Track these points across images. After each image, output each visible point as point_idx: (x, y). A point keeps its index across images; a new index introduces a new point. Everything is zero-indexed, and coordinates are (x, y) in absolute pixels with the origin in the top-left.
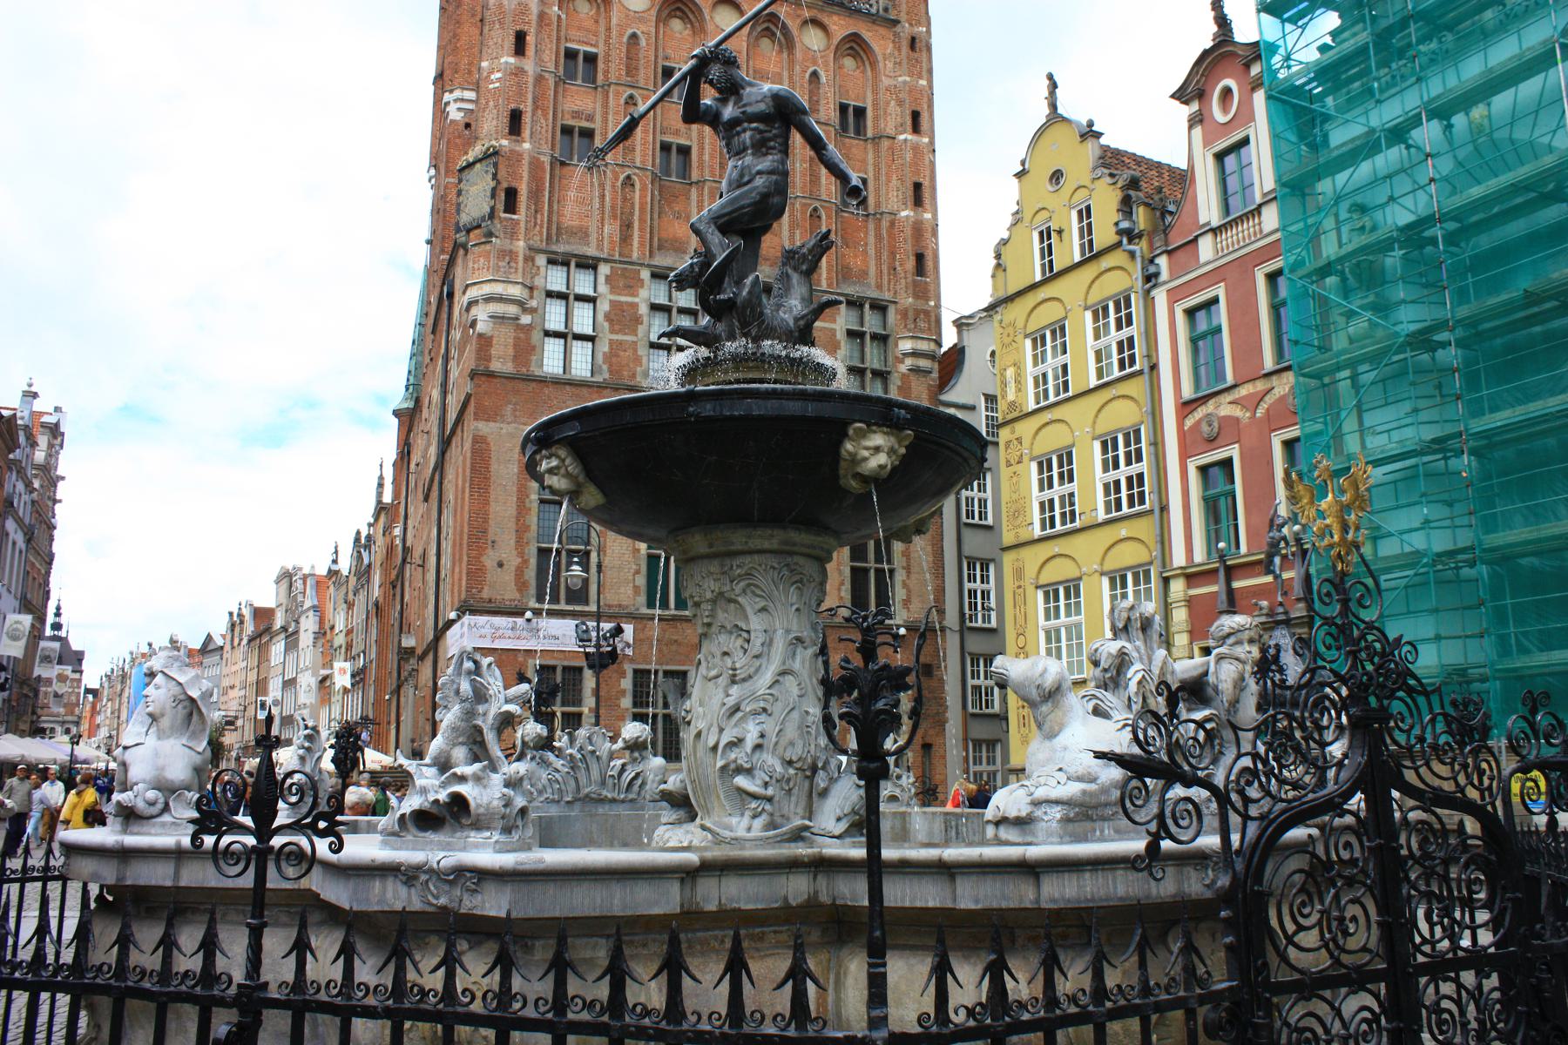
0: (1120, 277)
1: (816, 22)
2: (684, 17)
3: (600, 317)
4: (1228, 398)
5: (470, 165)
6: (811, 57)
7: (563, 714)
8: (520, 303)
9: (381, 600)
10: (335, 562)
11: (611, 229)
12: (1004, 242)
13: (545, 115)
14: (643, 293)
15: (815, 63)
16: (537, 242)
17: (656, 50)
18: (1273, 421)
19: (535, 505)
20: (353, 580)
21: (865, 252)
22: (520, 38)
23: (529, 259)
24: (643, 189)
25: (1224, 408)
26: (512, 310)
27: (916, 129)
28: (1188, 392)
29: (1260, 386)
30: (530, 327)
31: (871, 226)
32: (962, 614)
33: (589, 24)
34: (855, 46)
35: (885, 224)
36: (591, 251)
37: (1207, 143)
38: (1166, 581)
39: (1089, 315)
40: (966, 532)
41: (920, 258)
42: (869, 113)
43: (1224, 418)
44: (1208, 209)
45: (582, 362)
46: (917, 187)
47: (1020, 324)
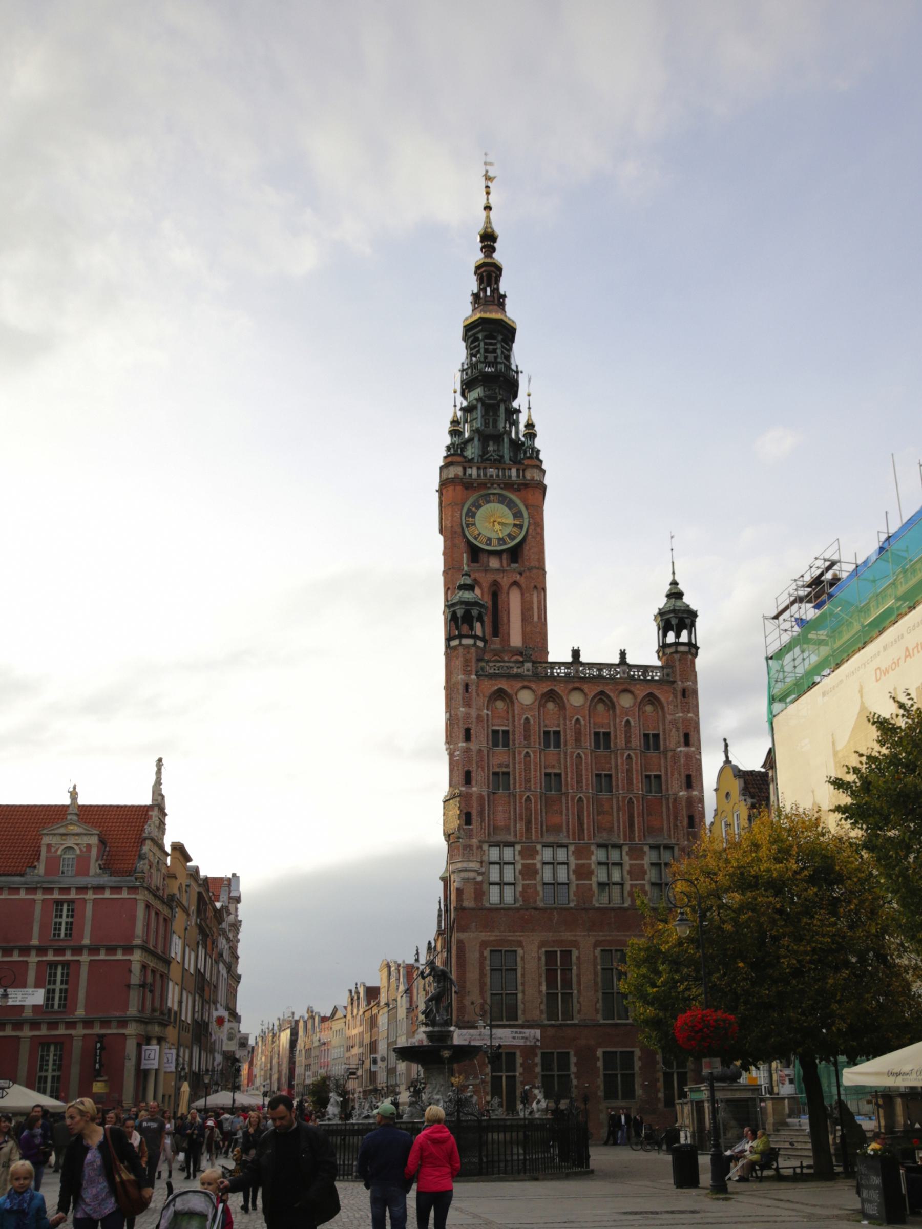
2: (554, 701)
6: (626, 711)
14: (539, 858)
15: (627, 715)
17: (539, 724)
23: (481, 847)
24: (536, 802)
26: (472, 875)
27: (687, 743)
30: (481, 883)
31: (664, 802)
34: (651, 699)
35: (671, 801)
36: (511, 839)
41: (691, 818)
42: (661, 737)
46: (689, 777)
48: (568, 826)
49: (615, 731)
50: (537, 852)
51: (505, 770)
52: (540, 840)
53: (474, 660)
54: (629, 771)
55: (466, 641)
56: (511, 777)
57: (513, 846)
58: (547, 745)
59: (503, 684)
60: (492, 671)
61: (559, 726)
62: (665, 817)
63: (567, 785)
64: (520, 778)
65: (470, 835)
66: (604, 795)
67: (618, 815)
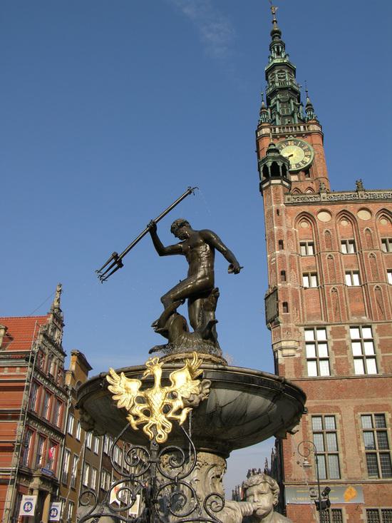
3: (330, 350)
8: (295, 349)
11: (331, 311)
13: (295, 271)
14: (347, 336)
26: (292, 352)
30: (300, 358)
36: (323, 322)
45: (325, 370)
51: (313, 271)
52: (347, 322)
53: (282, 193)
55: (273, 182)
57: (325, 329)
59: (306, 209)
60: (296, 201)
64: (326, 275)
65: (287, 320)
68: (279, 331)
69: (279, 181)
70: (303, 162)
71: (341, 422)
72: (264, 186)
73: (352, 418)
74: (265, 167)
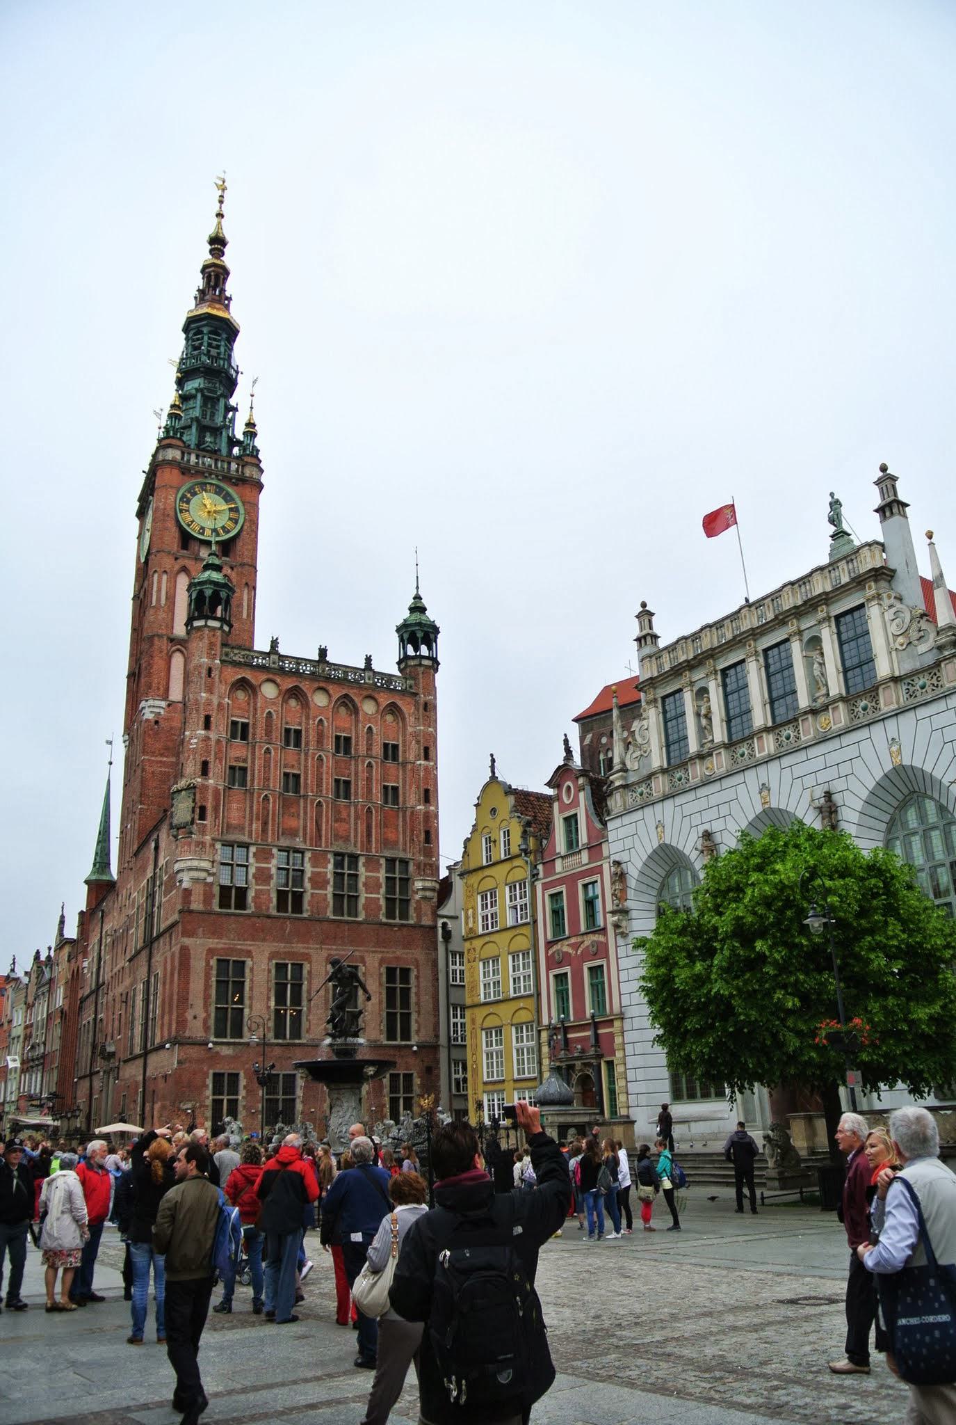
0: (521, 871)
1: (370, 697)
2: (297, 699)
3: (250, 877)
4: (566, 943)
5: (179, 791)
6: (369, 718)
7: (228, 1100)
9: (66, 1008)
10: (13, 970)
12: (467, 841)
13: (221, 762)
14: (274, 862)
16: (215, 835)
18: (586, 956)
19: (214, 984)
20: (32, 989)
21: (397, 829)
22: (208, 718)
24: (274, 802)
25: (565, 947)
26: (203, 875)
27: (427, 758)
28: (550, 937)
29: (579, 939)
32: (449, 1038)
33: (244, 705)
34: (393, 709)
35: (408, 813)
36: (246, 839)
37: (561, 812)
38: (539, 1032)
39: (507, 888)
40: (451, 989)
41: (427, 833)
42: (401, 748)
43: (567, 953)
44: (560, 845)
46: (427, 791)
47: (476, 885)
48: (305, 830)
49: (357, 737)
50: (272, 856)
51: (242, 764)
52: (276, 843)
53: (219, 644)
54: (369, 780)
55: (212, 623)
56: (249, 773)
58: (287, 743)
61: (300, 724)
62: (400, 829)
63: (306, 787)
66: (342, 802)
67: (356, 824)
68: (189, 844)
69: (216, 624)
70: (223, 528)
71: (252, 970)
72: (197, 624)
73: (264, 966)
74: (201, 593)
